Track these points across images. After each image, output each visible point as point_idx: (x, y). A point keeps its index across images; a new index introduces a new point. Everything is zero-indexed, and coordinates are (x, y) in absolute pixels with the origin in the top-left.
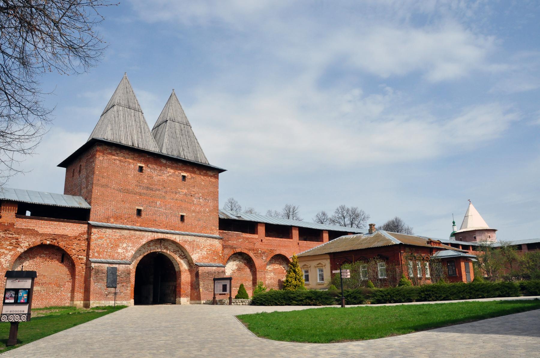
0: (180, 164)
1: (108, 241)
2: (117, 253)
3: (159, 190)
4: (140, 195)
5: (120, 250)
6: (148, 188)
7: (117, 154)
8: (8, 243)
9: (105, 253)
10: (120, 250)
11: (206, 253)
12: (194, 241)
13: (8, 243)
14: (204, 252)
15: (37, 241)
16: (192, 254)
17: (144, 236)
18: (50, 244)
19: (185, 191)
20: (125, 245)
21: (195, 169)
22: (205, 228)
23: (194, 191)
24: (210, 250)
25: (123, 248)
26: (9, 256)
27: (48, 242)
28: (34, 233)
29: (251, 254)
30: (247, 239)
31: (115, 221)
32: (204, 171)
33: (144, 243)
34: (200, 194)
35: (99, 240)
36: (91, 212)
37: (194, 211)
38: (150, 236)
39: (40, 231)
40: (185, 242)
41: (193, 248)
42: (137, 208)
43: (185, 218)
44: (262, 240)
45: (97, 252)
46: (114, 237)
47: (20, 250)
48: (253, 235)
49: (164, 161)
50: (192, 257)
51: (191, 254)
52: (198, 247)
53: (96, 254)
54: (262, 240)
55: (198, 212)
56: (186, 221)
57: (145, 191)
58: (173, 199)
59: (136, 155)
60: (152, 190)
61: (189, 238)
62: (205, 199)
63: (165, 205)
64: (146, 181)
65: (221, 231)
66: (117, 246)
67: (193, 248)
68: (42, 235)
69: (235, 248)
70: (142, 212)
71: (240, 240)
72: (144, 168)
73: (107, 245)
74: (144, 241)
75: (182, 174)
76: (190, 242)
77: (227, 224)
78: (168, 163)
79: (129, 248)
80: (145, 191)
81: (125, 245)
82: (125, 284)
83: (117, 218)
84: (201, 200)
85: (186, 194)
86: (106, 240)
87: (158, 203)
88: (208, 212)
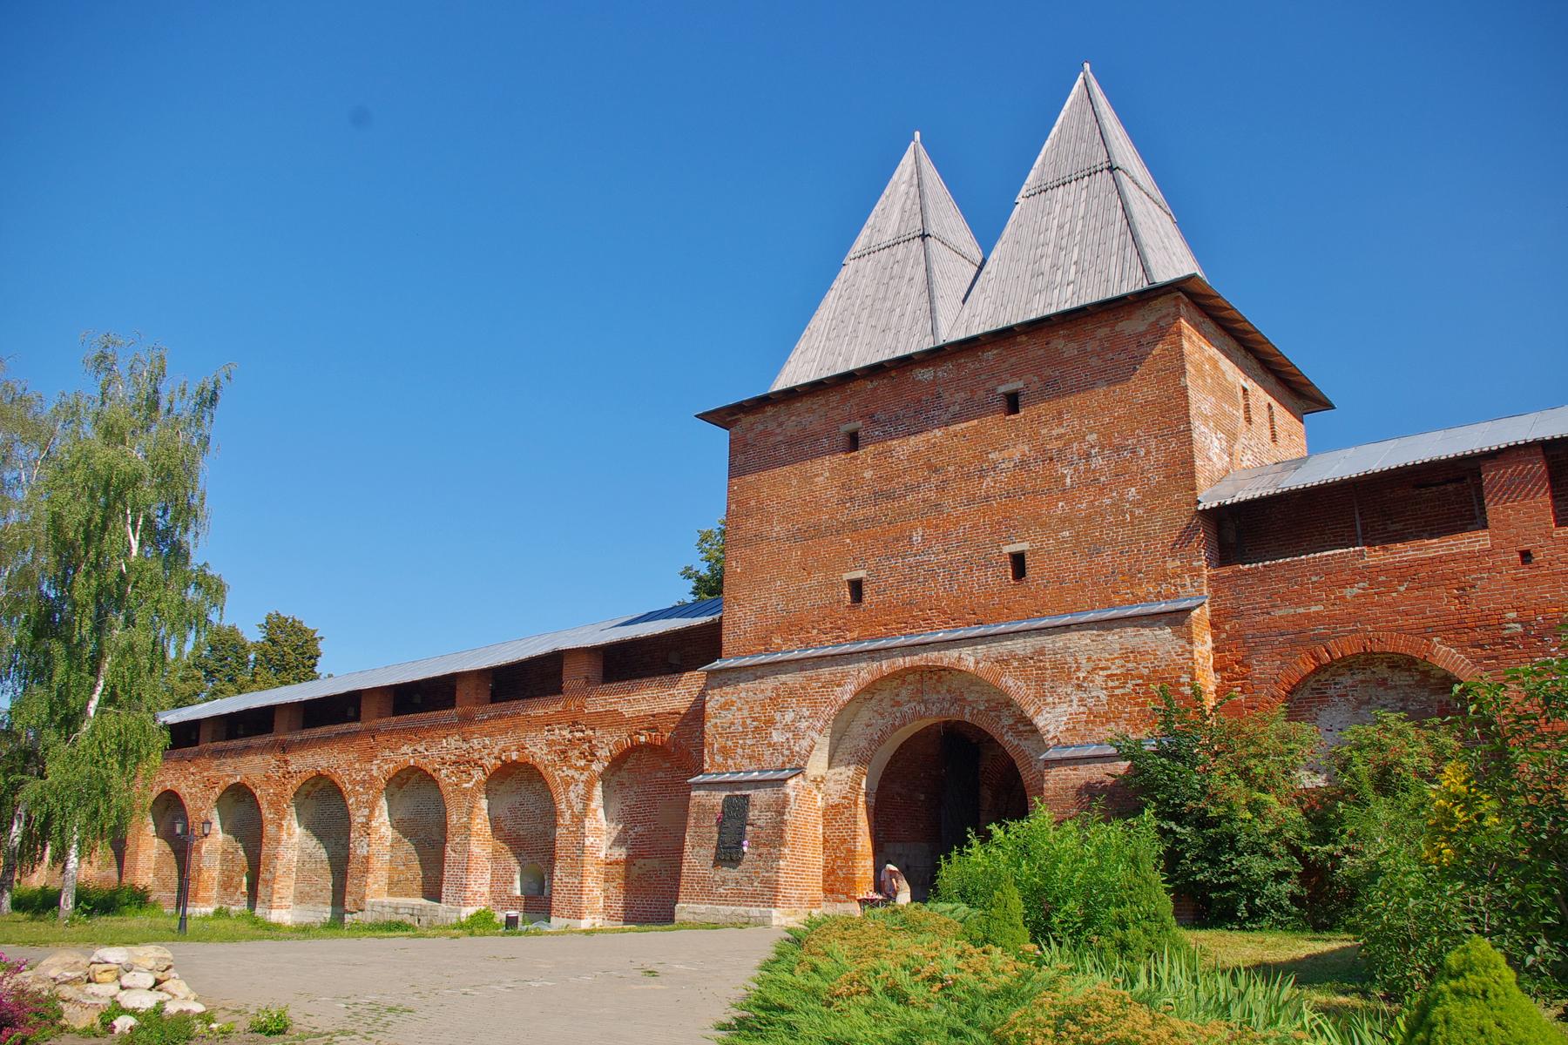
0: (991, 354)
1: (746, 713)
2: (769, 745)
3: (914, 489)
4: (854, 526)
5: (776, 737)
6: (878, 496)
7: (780, 425)
8: (576, 752)
9: (740, 751)
10: (776, 737)
11: (1103, 695)
12: (1041, 652)
13: (576, 752)
14: (1099, 692)
15: (622, 737)
16: (1039, 711)
17: (846, 675)
18: (647, 745)
19: (1020, 450)
20: (789, 716)
21: (1058, 343)
22: (1131, 577)
23: (1059, 437)
24: (1127, 676)
25: (787, 728)
26: (581, 785)
27: (642, 739)
28: (613, 720)
29: (1446, 655)
30: (1404, 573)
31: (785, 640)
32: (1103, 332)
33: (847, 697)
34: (1092, 438)
35: (724, 713)
36: (724, 631)
37: (1065, 520)
38: (864, 672)
39: (627, 711)
40: (1003, 662)
41: (1040, 681)
42: (847, 576)
43: (1028, 561)
44: (1526, 556)
45: (724, 751)
46: (761, 696)
47: (597, 767)
48: (1450, 541)
49: (925, 374)
50: (1040, 722)
51: (1030, 711)
52: (1063, 672)
53: (719, 759)
54: (1526, 556)
55: (1088, 518)
56: (1030, 573)
57: (870, 511)
58: (971, 500)
59: (834, 398)
60: (890, 497)
61: (1020, 646)
62: (1118, 449)
63: (946, 535)
64: (868, 474)
65: (1226, 571)
66: (771, 722)
67: (1040, 681)
68: (629, 721)
69: (1322, 638)
70: (865, 588)
71: (1349, 592)
72: (862, 434)
73: (744, 724)
74: (846, 692)
75: (1002, 389)
76: (1023, 660)
77: (1248, 532)
78: (945, 371)
79: (804, 724)
80: (870, 511)
81: (789, 716)
82: (764, 850)
83: (792, 627)
84: (1097, 462)
85: (1023, 464)
86: (740, 709)
87: (917, 538)
88: (1138, 504)
